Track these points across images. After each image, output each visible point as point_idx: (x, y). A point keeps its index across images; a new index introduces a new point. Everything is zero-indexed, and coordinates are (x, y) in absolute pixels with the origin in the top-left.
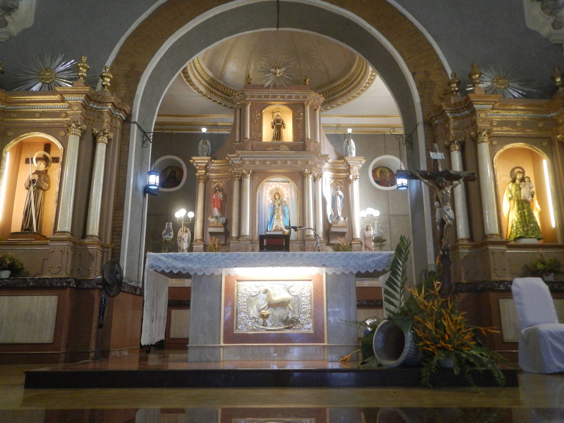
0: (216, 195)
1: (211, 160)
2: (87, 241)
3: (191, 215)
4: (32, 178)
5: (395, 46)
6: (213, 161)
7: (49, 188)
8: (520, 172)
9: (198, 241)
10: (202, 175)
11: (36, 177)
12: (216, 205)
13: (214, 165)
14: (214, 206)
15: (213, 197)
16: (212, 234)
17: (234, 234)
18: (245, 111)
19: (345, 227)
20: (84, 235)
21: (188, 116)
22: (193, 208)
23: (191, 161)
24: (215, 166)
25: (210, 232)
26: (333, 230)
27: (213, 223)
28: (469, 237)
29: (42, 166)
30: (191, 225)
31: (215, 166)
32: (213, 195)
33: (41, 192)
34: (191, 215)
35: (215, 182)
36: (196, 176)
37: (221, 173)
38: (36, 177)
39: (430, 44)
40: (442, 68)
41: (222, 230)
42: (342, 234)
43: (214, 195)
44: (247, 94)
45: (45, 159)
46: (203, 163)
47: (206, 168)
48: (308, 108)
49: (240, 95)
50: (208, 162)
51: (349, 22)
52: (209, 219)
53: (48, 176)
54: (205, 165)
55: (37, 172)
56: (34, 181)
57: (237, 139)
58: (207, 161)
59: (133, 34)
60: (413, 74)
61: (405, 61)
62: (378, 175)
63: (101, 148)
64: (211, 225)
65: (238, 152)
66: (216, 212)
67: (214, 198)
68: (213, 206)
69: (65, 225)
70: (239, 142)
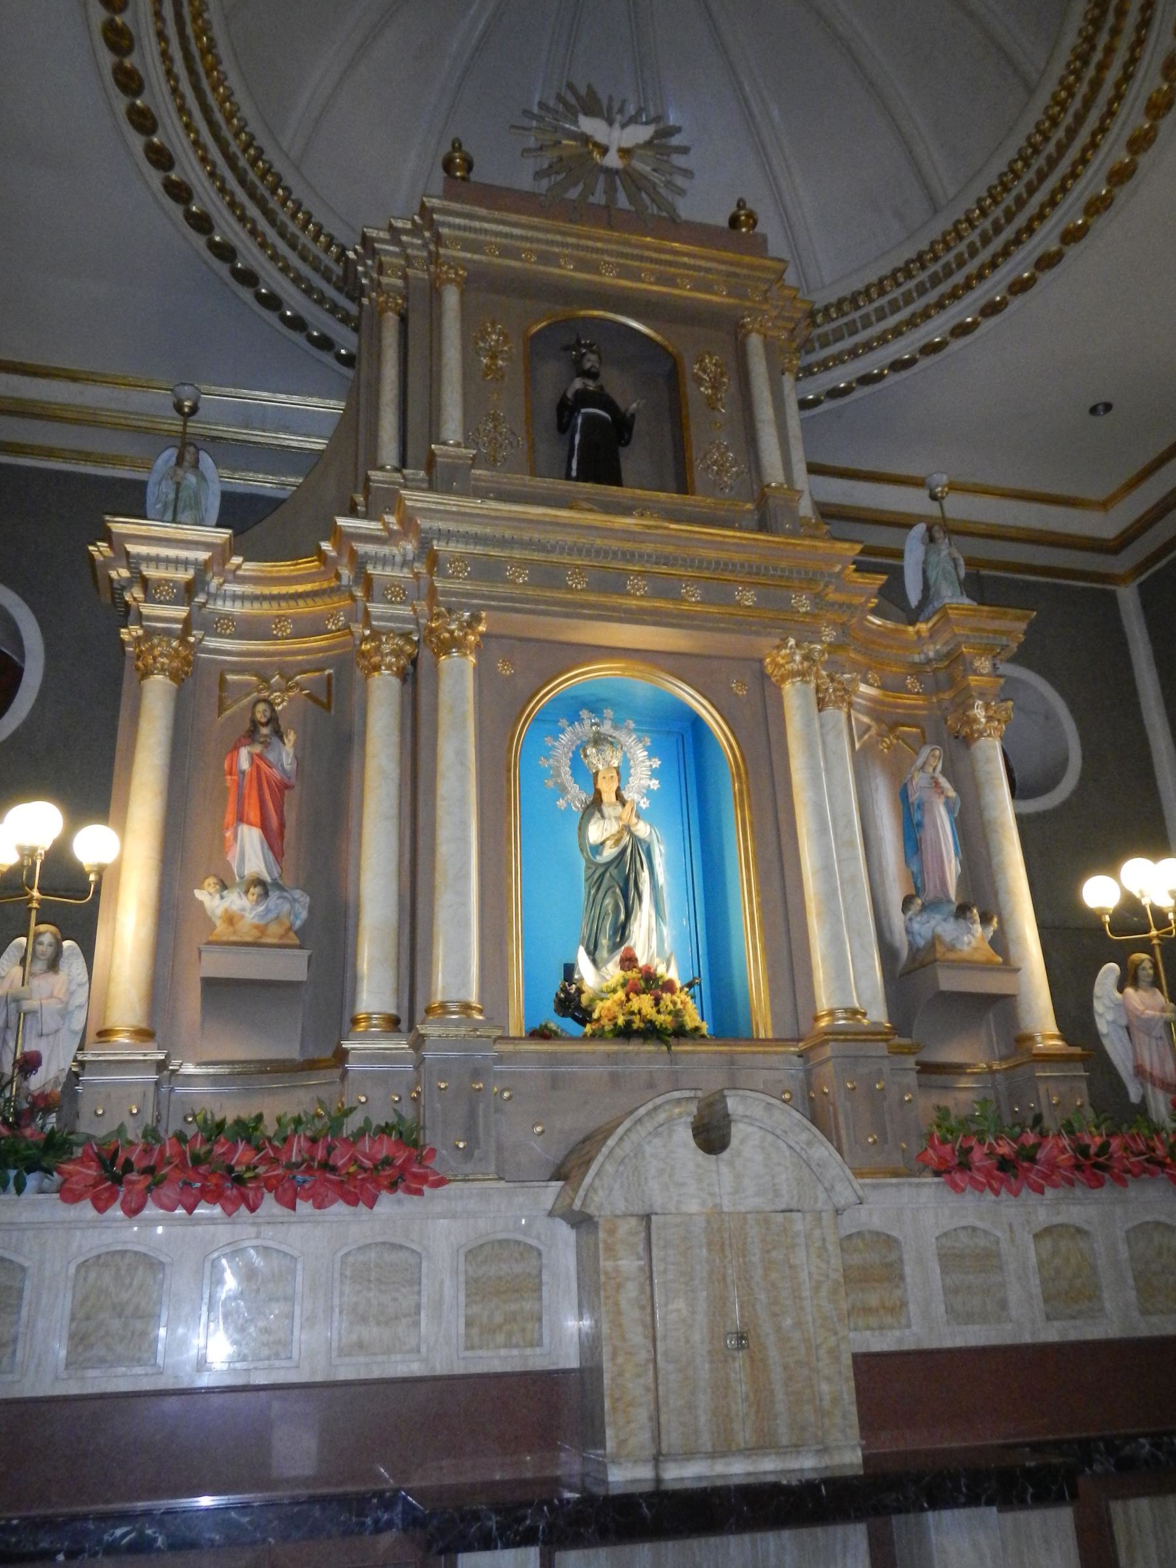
0: (257, 749)
1: (222, 553)
6: (237, 560)
9: (123, 1039)
10: (168, 633)
12: (253, 813)
13: (238, 589)
14: (241, 818)
15: (234, 761)
21: (72, 377)
23: (100, 550)
24: (243, 598)
25: (211, 986)
31: (243, 598)
32: (236, 748)
36: (123, 643)
37: (276, 638)
43: (244, 753)
44: (444, 231)
46: (177, 563)
49: (404, 238)
50: (207, 564)
52: (199, 894)
54: (189, 575)
58: (204, 556)
67: (244, 764)
68: (230, 816)
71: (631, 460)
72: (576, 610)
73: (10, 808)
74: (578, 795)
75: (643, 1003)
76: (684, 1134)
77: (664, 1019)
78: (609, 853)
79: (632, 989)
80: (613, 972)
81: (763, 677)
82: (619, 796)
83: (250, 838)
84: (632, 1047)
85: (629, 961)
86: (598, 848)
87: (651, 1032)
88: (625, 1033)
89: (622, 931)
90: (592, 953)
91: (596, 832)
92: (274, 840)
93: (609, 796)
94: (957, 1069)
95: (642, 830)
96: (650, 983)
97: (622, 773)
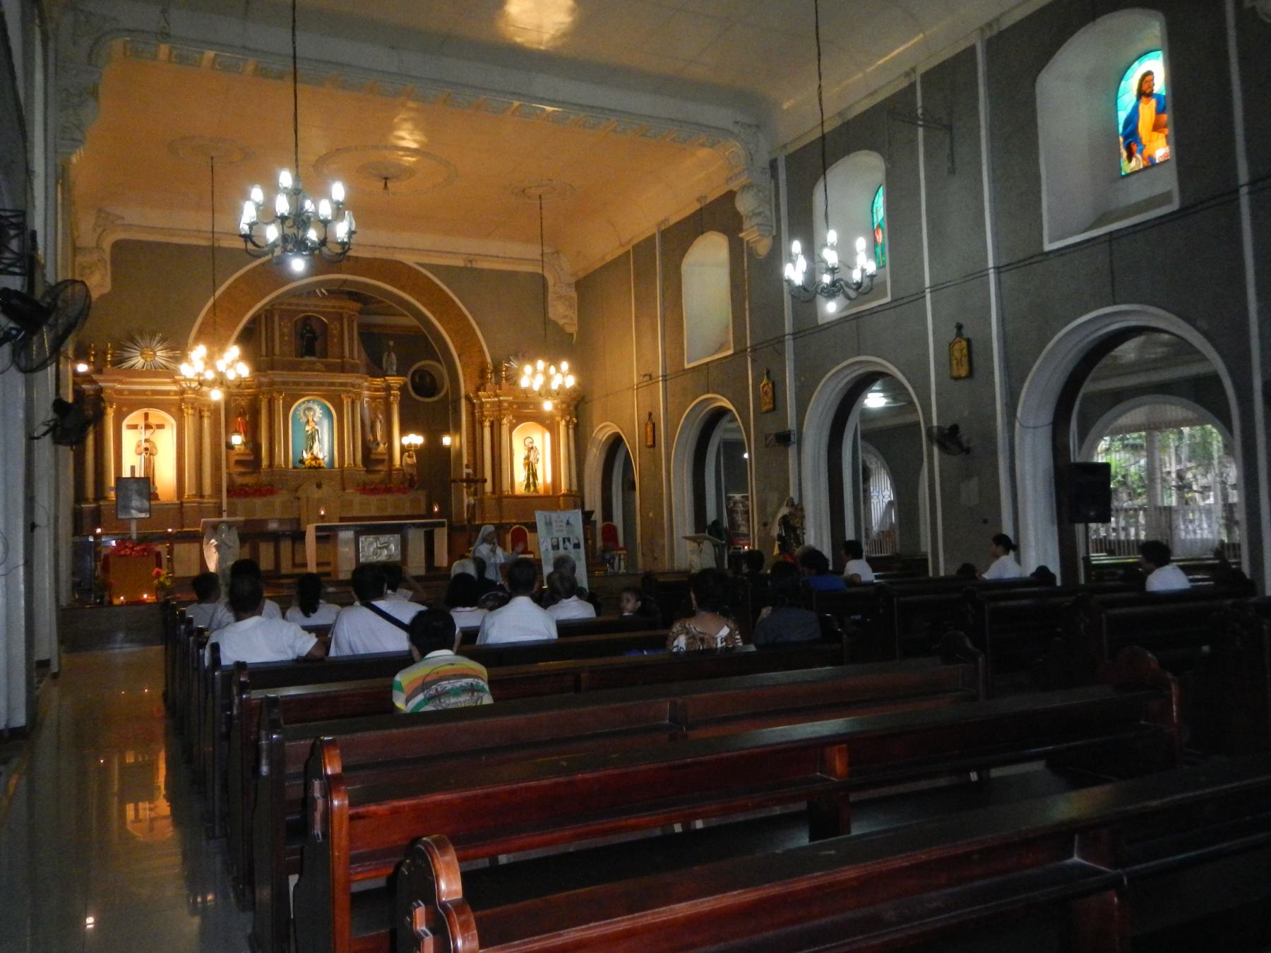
2: (205, 500)
4: (144, 445)
11: (147, 445)
16: (238, 462)
17: (265, 463)
18: (273, 322)
20: (202, 496)
26: (373, 457)
29: (149, 432)
39: (474, 330)
40: (481, 351)
41: (251, 458)
42: (382, 461)
45: (148, 427)
51: (407, 302)
53: (153, 443)
55: (146, 441)
56: (146, 449)
60: (459, 356)
61: (453, 343)
62: (417, 379)
63: (206, 422)
65: (269, 372)
71: (318, 345)
72: (301, 390)
74: (304, 420)
75: (313, 463)
76: (314, 486)
78: (310, 432)
80: (310, 455)
81: (341, 398)
82: (313, 421)
85: (312, 454)
87: (315, 467)
88: (310, 467)
89: (311, 448)
90: (306, 451)
91: (307, 428)
93: (311, 420)
94: (380, 471)
95: (317, 427)
96: (316, 458)
97: (314, 416)
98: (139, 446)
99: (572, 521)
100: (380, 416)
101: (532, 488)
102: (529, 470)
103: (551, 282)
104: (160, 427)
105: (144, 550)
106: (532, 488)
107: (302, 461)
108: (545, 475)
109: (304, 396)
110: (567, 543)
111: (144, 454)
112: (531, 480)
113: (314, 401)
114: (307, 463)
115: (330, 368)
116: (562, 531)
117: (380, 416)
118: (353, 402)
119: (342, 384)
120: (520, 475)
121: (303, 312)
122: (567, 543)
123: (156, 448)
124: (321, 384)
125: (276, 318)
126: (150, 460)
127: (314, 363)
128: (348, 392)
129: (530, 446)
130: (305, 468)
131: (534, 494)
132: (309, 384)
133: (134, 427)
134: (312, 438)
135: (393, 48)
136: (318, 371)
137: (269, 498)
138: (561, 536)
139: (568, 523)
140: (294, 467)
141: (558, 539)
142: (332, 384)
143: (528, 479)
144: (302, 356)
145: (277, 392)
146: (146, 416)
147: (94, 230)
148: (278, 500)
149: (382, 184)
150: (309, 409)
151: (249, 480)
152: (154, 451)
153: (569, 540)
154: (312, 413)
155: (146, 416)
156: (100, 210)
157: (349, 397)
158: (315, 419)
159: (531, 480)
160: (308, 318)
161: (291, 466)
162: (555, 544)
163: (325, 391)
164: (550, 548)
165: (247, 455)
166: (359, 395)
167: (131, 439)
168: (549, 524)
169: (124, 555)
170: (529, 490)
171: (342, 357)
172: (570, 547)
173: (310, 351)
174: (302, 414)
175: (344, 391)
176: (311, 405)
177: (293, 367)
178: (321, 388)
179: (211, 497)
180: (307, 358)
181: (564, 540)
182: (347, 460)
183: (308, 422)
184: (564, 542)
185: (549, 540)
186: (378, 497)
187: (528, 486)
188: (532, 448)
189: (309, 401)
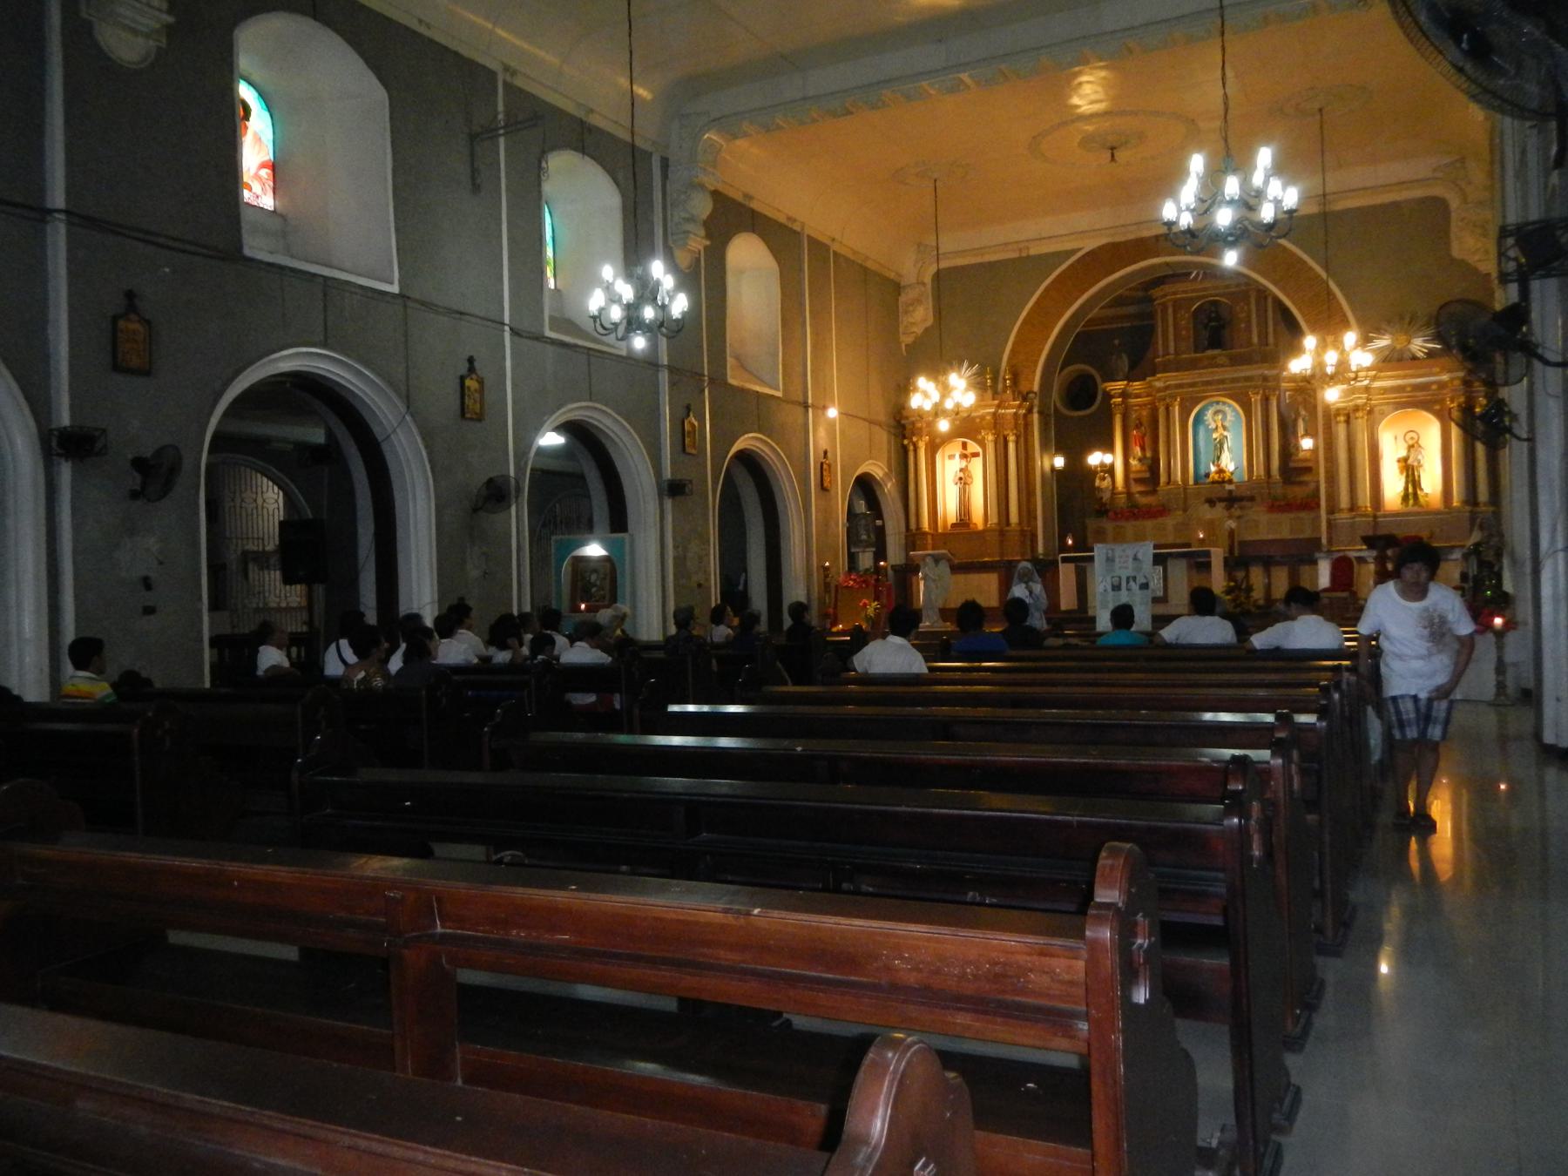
3: (1108, 458)
5: (1294, 303)
7: (972, 482)
8: (1412, 438)
11: (962, 475)
14: (1136, 445)
16: (1138, 481)
17: (1163, 479)
19: (1306, 460)
20: (1008, 524)
22: (1108, 447)
26: (1292, 465)
27: (1135, 465)
28: (1349, 506)
29: (964, 464)
30: (1110, 470)
33: (967, 486)
34: (1108, 458)
35: (1136, 411)
38: (962, 475)
41: (1147, 475)
45: (964, 456)
47: (1124, 395)
48: (1253, 301)
53: (970, 472)
55: (961, 470)
56: (961, 479)
57: (1161, 353)
59: (1025, 322)
63: (1011, 447)
64: (1134, 469)
66: (1137, 451)
69: (993, 519)
70: (1163, 356)
72: (1199, 392)
73: (1095, 451)
74: (1213, 426)
77: (1220, 480)
79: (1217, 472)
83: (1138, 449)
84: (1215, 485)
85: (1218, 466)
86: (1216, 439)
87: (1217, 482)
89: (1219, 458)
90: (1213, 463)
91: (1215, 436)
92: (1143, 449)
95: (1225, 433)
96: (1221, 471)
98: (956, 476)
99: (1140, 556)
100: (1303, 412)
101: (1411, 502)
102: (1407, 476)
103: (1454, 204)
104: (975, 455)
105: (864, 582)
106: (1411, 502)
107: (1207, 475)
108: (1431, 482)
109: (1196, 401)
110: (1132, 583)
111: (959, 484)
112: (1410, 490)
113: (1224, 403)
114: (1211, 476)
115: (1236, 361)
116: (1126, 568)
117: (1303, 412)
118: (1266, 400)
119: (1247, 379)
120: (1393, 487)
121: (1199, 298)
122: (1132, 583)
123: (971, 477)
124: (1222, 381)
125: (1170, 310)
126: (965, 491)
127: (1214, 357)
128: (1256, 387)
129: (1411, 442)
130: (1209, 483)
131: (1416, 509)
132: (1208, 383)
133: (951, 457)
134: (1219, 446)
135: (940, 41)
136: (1222, 366)
137: (1160, 520)
138: (1124, 574)
139: (1135, 558)
140: (1196, 483)
141: (1120, 578)
142: (1234, 380)
143: (1406, 489)
144: (1203, 352)
145: (1170, 397)
146: (964, 446)
147: (915, 265)
148: (1170, 522)
149: (1109, 155)
150: (1216, 413)
151: (1143, 500)
152: (969, 481)
153: (1134, 579)
154: (1220, 417)
155: (964, 446)
156: (919, 245)
157: (1257, 393)
158: (1227, 424)
159: (1410, 490)
160: (1215, 303)
161: (1191, 482)
162: (1116, 583)
163: (1230, 389)
164: (1109, 588)
165: (1145, 471)
166: (1277, 388)
167: (949, 467)
168: (1110, 560)
169: (847, 587)
170: (1407, 505)
171: (1250, 343)
172: (1134, 587)
173: (1216, 341)
174: (1211, 420)
175: (1250, 387)
176: (1220, 407)
177: (1193, 365)
178: (1221, 386)
179: (1020, 523)
180: (1210, 352)
181: (1128, 578)
182: (1259, 470)
183: (1217, 428)
184: (1128, 582)
185: (1109, 579)
186: (1292, 515)
187: (1405, 498)
188: (1412, 446)
189: (1218, 403)
